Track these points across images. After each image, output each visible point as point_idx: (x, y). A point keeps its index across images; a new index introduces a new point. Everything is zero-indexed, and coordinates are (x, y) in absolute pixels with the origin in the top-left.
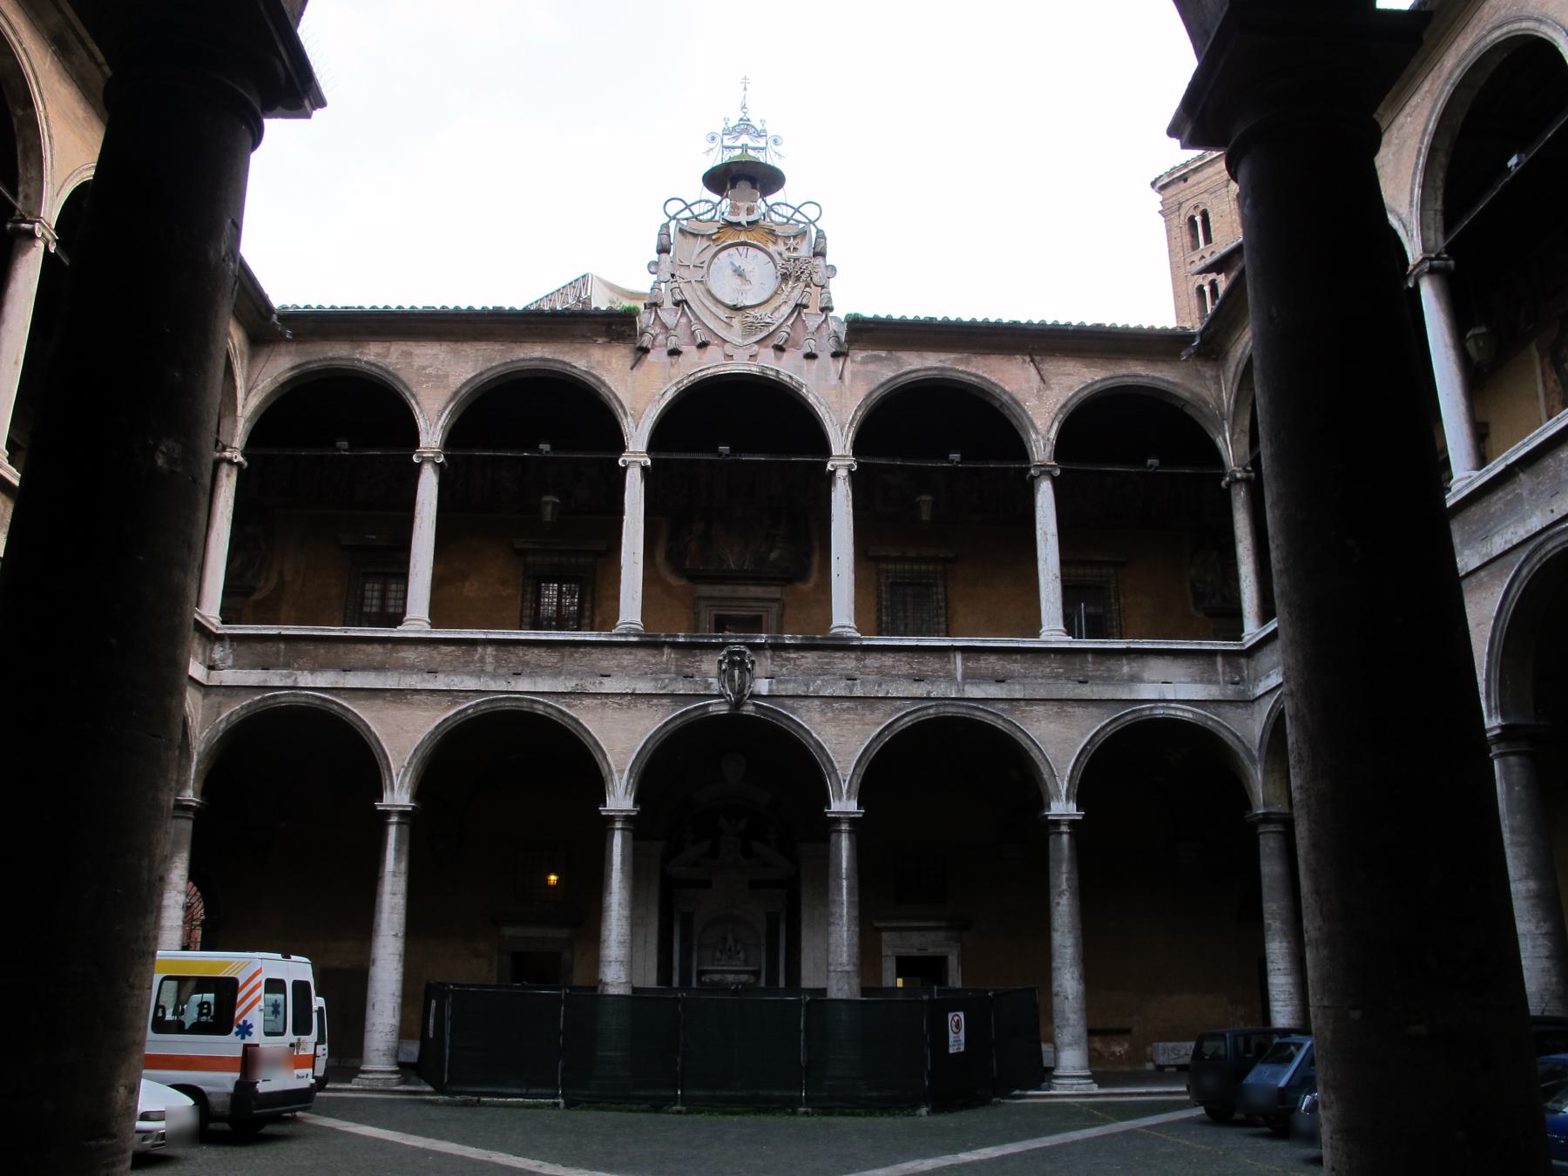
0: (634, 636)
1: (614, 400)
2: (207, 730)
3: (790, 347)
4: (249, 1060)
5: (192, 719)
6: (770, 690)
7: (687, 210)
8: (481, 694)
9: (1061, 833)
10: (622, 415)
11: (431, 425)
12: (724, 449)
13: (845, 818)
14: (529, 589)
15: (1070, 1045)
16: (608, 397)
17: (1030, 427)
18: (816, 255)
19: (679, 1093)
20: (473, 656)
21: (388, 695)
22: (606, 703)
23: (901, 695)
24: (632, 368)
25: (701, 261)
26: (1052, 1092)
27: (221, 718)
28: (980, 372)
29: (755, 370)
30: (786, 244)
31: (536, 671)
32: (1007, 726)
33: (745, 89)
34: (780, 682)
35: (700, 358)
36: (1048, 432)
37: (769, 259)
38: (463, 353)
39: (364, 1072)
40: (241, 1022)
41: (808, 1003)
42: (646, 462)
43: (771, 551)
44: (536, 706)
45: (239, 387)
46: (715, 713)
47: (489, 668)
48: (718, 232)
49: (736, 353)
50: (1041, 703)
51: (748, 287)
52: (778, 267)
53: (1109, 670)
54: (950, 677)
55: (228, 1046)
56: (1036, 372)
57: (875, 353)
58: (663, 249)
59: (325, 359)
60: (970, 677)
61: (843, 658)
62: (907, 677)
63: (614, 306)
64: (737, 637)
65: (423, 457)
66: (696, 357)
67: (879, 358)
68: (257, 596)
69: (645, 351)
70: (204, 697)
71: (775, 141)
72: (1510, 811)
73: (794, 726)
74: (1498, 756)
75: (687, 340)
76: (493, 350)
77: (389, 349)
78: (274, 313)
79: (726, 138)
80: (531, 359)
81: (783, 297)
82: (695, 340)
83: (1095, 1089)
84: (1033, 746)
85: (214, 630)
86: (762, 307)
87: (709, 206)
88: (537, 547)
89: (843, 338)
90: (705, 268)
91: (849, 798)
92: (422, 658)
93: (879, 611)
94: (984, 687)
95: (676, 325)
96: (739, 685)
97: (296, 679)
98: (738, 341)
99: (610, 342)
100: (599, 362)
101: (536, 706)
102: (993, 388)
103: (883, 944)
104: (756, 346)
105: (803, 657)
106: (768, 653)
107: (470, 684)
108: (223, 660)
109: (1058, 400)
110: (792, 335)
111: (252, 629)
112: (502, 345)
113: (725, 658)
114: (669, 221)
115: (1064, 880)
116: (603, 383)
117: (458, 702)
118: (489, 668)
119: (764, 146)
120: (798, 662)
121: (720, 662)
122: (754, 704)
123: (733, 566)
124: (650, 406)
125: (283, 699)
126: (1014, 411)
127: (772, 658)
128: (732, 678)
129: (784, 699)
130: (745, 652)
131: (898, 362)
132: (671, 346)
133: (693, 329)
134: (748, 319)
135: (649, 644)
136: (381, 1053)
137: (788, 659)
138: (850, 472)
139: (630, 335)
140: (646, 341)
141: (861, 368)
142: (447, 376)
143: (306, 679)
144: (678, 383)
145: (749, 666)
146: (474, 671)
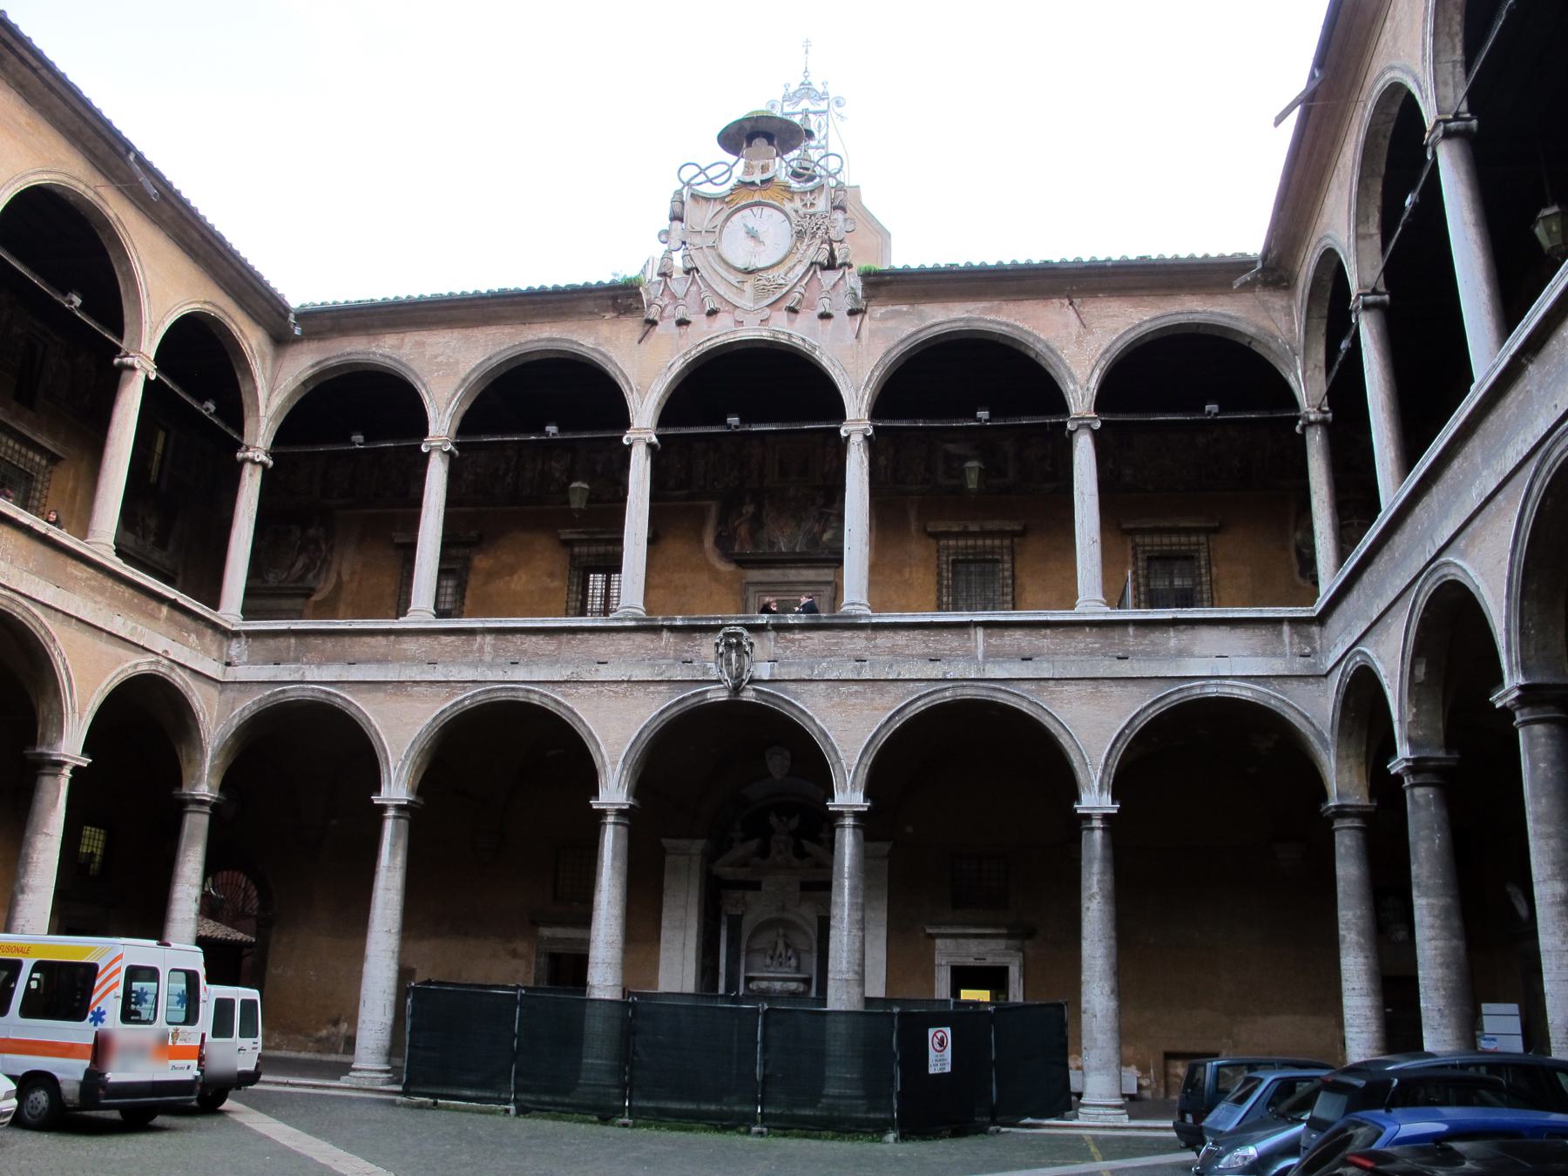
0: (631, 620)
1: (620, 377)
2: (221, 725)
4: (101, 1048)
5: (204, 714)
6: (771, 675)
7: (702, 175)
8: (479, 684)
9: (1092, 829)
10: (628, 391)
11: (439, 414)
12: (733, 420)
13: (848, 812)
14: (575, 580)
15: (1097, 1069)
16: (615, 373)
17: (1066, 376)
18: (835, 208)
19: (627, 1104)
20: (472, 645)
21: (390, 687)
22: (602, 691)
23: (914, 677)
24: (640, 342)
26: (1075, 1122)
27: (234, 713)
28: (1011, 321)
29: (765, 335)
30: (802, 200)
31: (534, 659)
32: (1032, 708)
33: (807, 52)
34: (782, 665)
35: (709, 327)
36: (1088, 381)
37: (784, 218)
38: (473, 339)
39: (354, 1070)
40: (95, 1009)
41: (766, 1012)
42: (651, 438)
43: (824, 531)
44: (532, 696)
45: (259, 387)
46: (713, 700)
47: (488, 658)
48: (731, 194)
49: (747, 319)
50: (1073, 682)
51: (762, 248)
53: (1153, 643)
54: (970, 656)
55: (80, 1033)
56: (1076, 315)
57: (897, 307)
58: (676, 217)
59: (343, 355)
60: (992, 655)
61: (852, 638)
62: (921, 657)
63: (617, 279)
64: (737, 619)
65: (431, 447)
66: (706, 326)
67: (900, 313)
68: (316, 598)
69: (653, 323)
70: (221, 692)
71: (837, 102)
72: (1534, 796)
73: (797, 713)
74: (1525, 723)
75: (697, 309)
76: (503, 334)
77: (403, 340)
78: (291, 312)
79: (786, 104)
80: (539, 340)
81: (798, 255)
83: (1125, 1120)
84: (1062, 731)
85: (230, 627)
87: (726, 168)
88: (584, 537)
90: (717, 232)
91: (854, 790)
92: (424, 649)
93: (939, 591)
94: (1007, 665)
95: (685, 296)
96: (737, 669)
97: (304, 673)
98: (749, 305)
99: (617, 317)
100: (606, 338)
101: (532, 696)
102: (1026, 337)
103: (937, 952)
104: (768, 310)
105: (809, 638)
106: (772, 635)
107: (469, 674)
108: (239, 657)
109: (1100, 346)
110: (806, 295)
111: (264, 624)
112: (512, 328)
113: (721, 640)
114: (683, 188)
115: (1095, 882)
116: (610, 359)
117: (456, 693)
118: (488, 658)
119: (825, 108)
120: (803, 644)
121: (717, 645)
122: (754, 690)
123: (783, 549)
124: (656, 380)
125: (291, 694)
126: (1048, 359)
127: (776, 642)
128: (729, 663)
129: (788, 683)
130: (742, 634)
131: (921, 317)
132: (678, 316)
135: (648, 629)
136: (370, 1051)
137: (792, 641)
138: (866, 437)
139: (637, 308)
140: (653, 313)
141: (880, 325)
142: (458, 362)
143: (313, 673)
144: (686, 354)
145: (748, 649)
146: (473, 662)
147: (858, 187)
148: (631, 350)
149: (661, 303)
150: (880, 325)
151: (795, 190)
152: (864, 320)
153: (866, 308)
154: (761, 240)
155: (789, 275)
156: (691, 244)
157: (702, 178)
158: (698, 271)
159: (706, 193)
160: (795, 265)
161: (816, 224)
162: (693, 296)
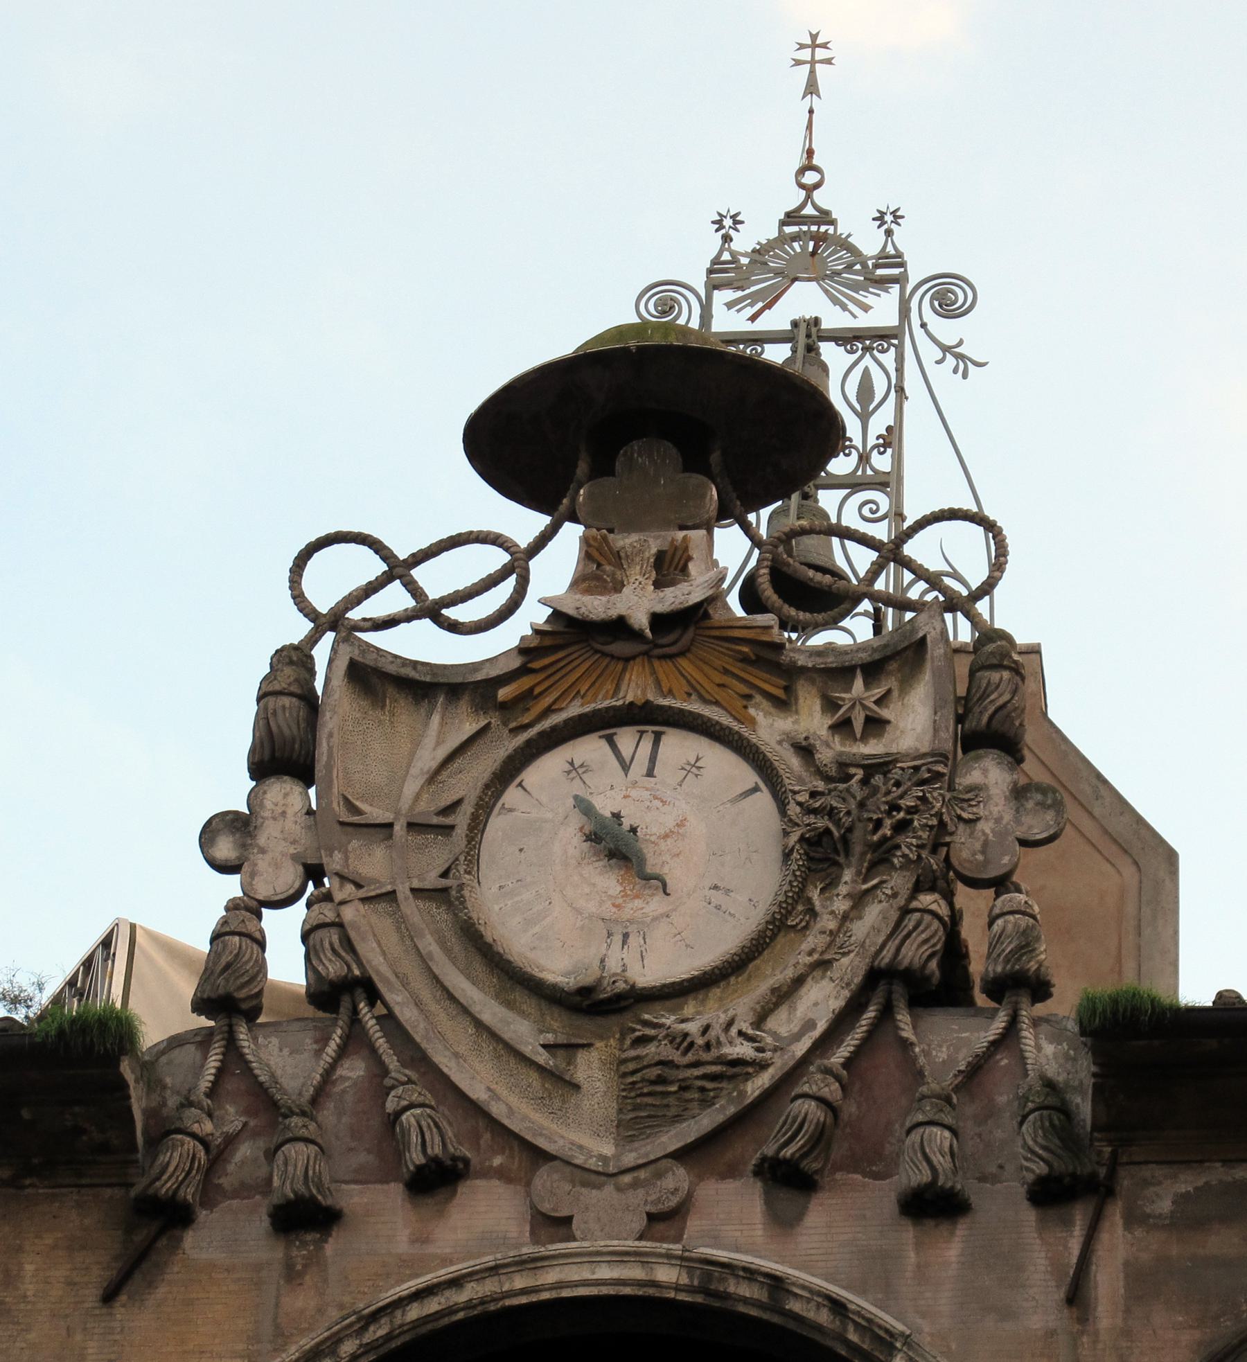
3: (838, 1168)
24: (109, 1297)
25: (447, 799)
30: (830, 705)
33: (812, 88)
35: (421, 1239)
37: (747, 776)
48: (522, 671)
51: (655, 905)
52: (794, 810)
75: (363, 1158)
79: (721, 297)
81: (813, 940)
82: (399, 1153)
86: (716, 992)
87: (497, 558)
89: (1084, 1107)
90: (461, 831)
95: (314, 1101)
104: (681, 1171)
110: (850, 1109)
132: (285, 1186)
133: (391, 1105)
134: (651, 1049)
141: (1174, 1251)
147: (1039, 645)
148: (69, 1332)
149: (208, 1127)
150: (1174, 1251)
151: (802, 661)
152: (1106, 1224)
153: (1112, 1173)
154: (649, 869)
155: (771, 1023)
156: (343, 878)
157: (395, 599)
158: (373, 995)
159: (415, 664)
160: (799, 982)
161: (894, 807)
162: (349, 1098)
